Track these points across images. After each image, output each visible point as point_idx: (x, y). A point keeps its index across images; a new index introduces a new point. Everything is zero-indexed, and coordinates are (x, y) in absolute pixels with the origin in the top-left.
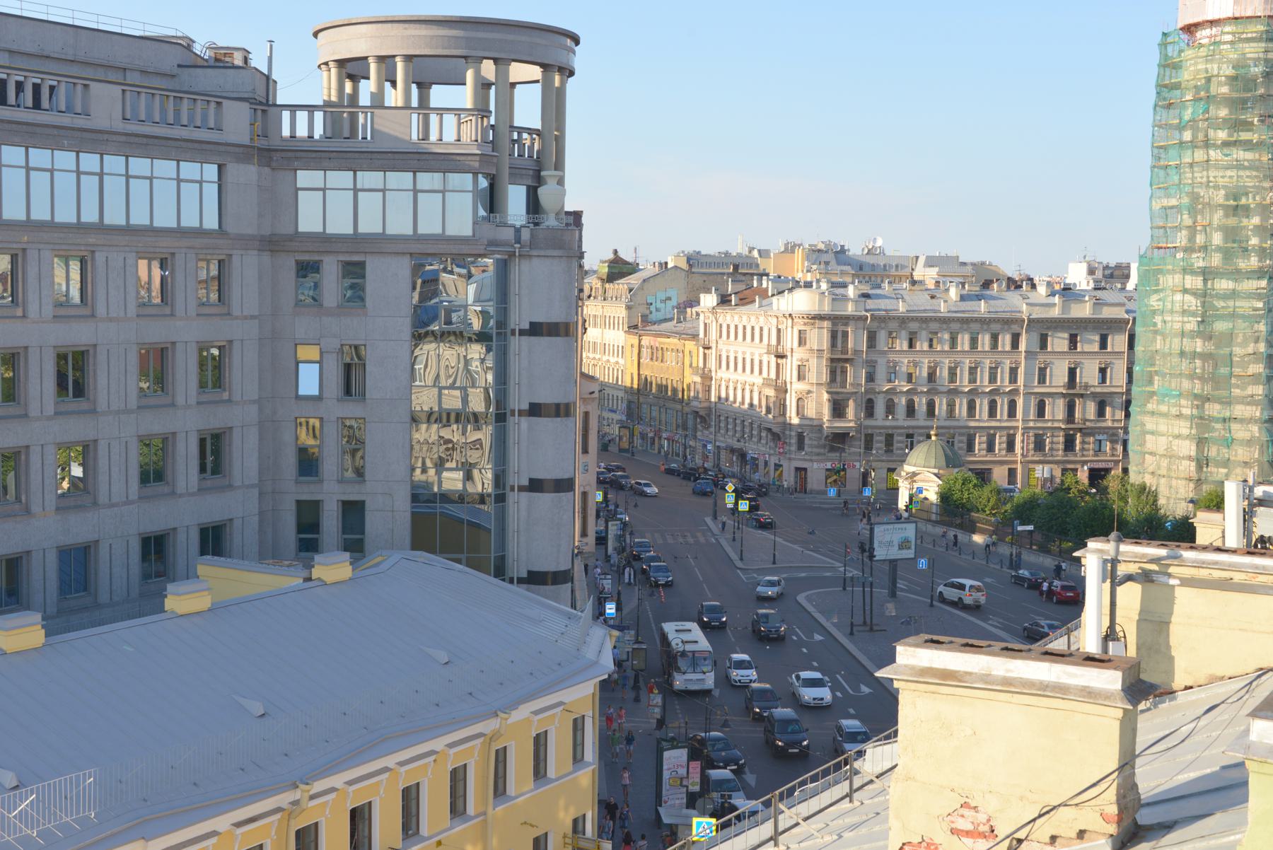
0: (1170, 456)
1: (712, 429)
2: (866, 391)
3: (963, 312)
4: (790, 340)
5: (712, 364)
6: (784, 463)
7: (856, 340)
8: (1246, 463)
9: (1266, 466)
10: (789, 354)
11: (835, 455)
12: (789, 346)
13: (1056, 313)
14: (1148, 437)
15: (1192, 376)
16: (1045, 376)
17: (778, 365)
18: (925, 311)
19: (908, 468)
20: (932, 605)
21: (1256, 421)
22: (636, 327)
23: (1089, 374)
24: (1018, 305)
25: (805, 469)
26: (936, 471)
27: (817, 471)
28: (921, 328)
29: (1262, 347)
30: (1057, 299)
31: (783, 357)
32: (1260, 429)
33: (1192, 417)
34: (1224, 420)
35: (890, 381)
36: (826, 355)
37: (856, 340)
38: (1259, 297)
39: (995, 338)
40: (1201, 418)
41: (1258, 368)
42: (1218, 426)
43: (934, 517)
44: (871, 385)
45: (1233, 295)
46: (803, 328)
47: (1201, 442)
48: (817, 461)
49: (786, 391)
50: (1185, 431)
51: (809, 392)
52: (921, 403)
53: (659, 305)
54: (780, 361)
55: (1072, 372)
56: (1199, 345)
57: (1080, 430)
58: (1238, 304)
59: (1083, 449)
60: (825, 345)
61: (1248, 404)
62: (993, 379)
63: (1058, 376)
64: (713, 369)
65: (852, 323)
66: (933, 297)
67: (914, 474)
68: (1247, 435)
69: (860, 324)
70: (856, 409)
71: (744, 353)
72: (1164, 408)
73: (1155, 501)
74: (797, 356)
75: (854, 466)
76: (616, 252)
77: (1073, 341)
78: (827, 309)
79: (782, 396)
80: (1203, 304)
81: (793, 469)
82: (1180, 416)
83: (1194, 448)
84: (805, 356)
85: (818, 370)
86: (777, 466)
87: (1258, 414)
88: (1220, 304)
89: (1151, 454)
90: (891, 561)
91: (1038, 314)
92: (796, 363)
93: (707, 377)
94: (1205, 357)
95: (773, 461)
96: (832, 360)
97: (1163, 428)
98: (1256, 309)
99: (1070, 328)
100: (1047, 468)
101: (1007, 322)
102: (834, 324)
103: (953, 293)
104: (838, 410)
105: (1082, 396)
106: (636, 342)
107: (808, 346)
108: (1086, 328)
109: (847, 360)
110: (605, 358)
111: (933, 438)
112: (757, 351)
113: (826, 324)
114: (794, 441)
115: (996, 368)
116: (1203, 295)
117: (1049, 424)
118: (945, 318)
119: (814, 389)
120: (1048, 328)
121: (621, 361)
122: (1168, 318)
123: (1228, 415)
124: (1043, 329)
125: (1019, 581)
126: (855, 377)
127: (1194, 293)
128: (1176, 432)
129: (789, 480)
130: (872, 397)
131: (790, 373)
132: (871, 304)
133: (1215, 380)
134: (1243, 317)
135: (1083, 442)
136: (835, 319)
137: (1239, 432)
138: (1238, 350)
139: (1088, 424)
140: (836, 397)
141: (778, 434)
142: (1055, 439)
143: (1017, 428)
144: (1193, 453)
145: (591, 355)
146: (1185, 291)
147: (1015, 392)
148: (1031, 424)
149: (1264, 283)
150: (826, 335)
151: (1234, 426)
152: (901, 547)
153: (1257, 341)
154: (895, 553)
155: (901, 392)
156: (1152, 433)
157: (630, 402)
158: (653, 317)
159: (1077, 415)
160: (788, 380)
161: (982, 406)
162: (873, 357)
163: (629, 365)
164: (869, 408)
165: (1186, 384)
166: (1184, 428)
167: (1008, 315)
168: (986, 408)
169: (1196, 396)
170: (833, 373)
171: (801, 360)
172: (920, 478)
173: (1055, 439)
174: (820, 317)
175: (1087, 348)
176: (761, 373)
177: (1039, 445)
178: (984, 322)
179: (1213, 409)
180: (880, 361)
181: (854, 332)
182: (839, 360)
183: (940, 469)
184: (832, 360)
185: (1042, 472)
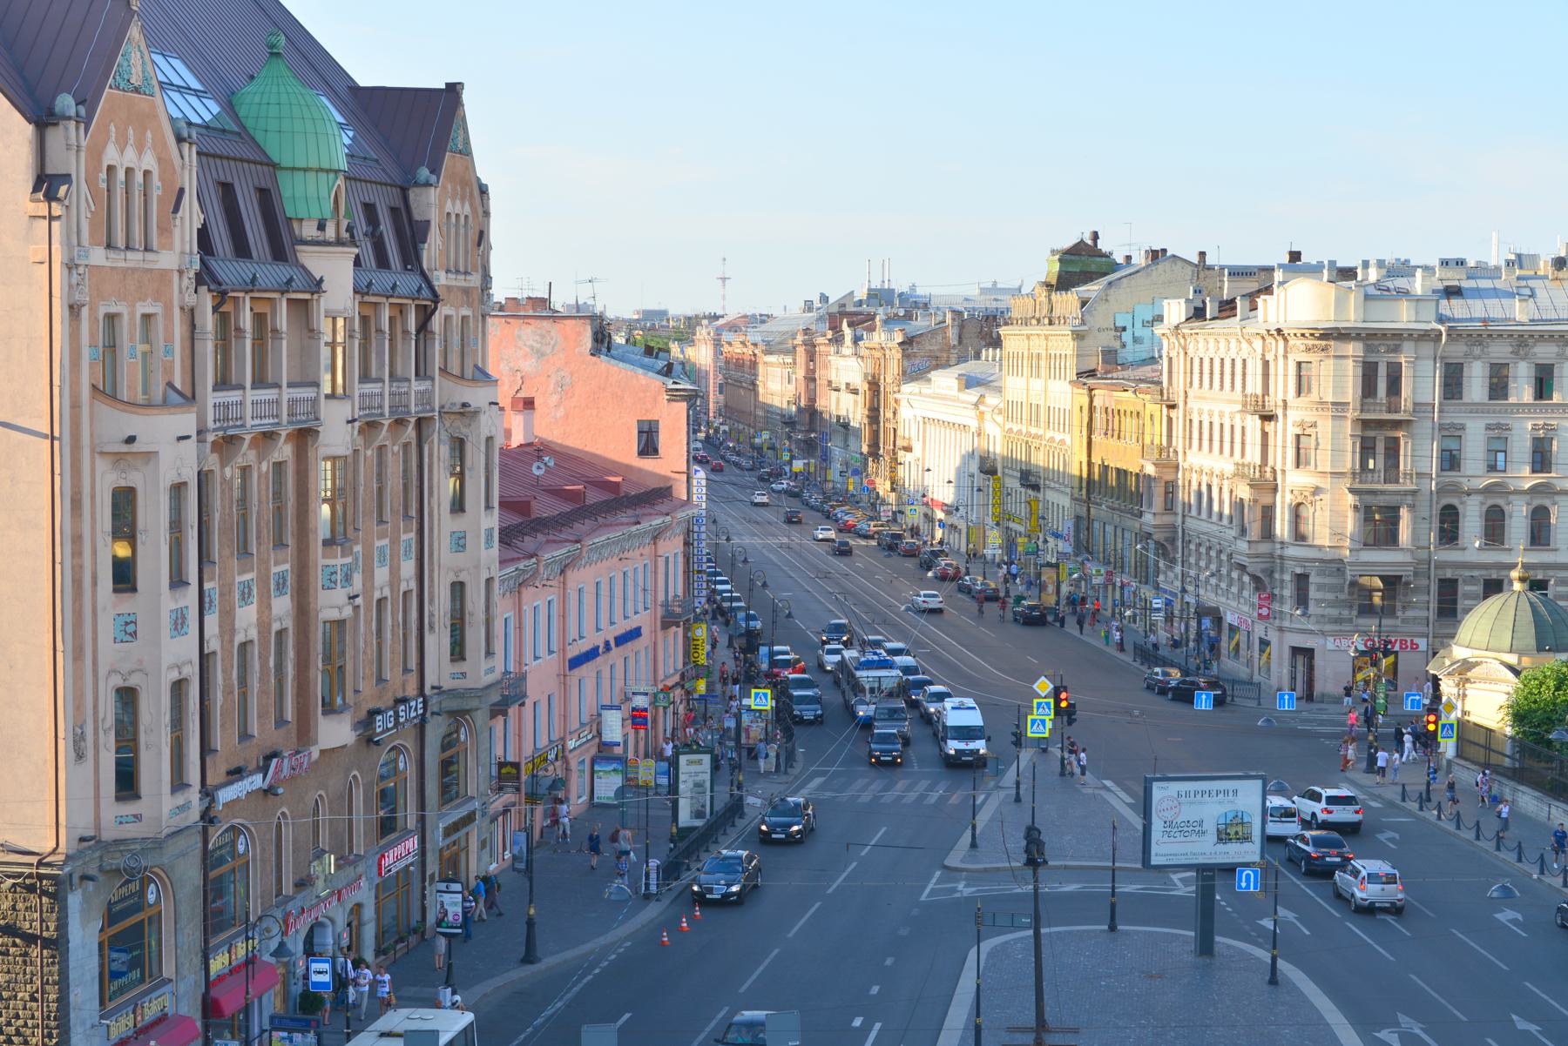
1: (1178, 569)
4: (1283, 385)
5: (1178, 442)
6: (1273, 637)
10: (1280, 412)
11: (1372, 624)
12: (1280, 397)
17: (1265, 435)
19: (1459, 652)
20: (1273, 980)
22: (1092, 373)
25: (1308, 653)
26: (1512, 659)
27: (1337, 655)
31: (1267, 418)
35: (1492, 468)
36: (1351, 414)
37: (1421, 383)
43: (1507, 762)
44: (1451, 476)
46: (1303, 357)
48: (1335, 634)
49: (1275, 489)
51: (1317, 491)
53: (1140, 331)
54: (1270, 427)
60: (1351, 392)
64: (1180, 450)
65: (1408, 347)
67: (1467, 666)
69: (1427, 348)
70: (1415, 521)
71: (1221, 416)
74: (1294, 415)
75: (1414, 647)
76: (1095, 236)
78: (1352, 317)
79: (1266, 500)
81: (1287, 654)
84: (1309, 417)
85: (1335, 445)
86: (1264, 643)
90: (1202, 869)
92: (1292, 431)
93: (1168, 463)
95: (1259, 631)
96: (1365, 424)
102: (1369, 349)
104: (1379, 524)
106: (1085, 401)
107: (1314, 396)
109: (1397, 424)
110: (1049, 434)
112: (1216, 405)
113: (1353, 349)
114: (1288, 592)
119: (1325, 483)
121: (1068, 442)
126: (1419, 456)
129: (1280, 668)
130: (1455, 501)
131: (1281, 455)
136: (1369, 337)
140: (1369, 499)
141: (1276, 574)
145: (1033, 430)
150: (1351, 374)
152: (1223, 836)
154: (1209, 851)
157: (1078, 518)
158: (1128, 354)
160: (1278, 468)
163: (1076, 448)
170: (1367, 449)
171: (1301, 424)
176: (1232, 454)
181: (1413, 364)
182: (1381, 424)
183: (1521, 654)
184: (1365, 424)
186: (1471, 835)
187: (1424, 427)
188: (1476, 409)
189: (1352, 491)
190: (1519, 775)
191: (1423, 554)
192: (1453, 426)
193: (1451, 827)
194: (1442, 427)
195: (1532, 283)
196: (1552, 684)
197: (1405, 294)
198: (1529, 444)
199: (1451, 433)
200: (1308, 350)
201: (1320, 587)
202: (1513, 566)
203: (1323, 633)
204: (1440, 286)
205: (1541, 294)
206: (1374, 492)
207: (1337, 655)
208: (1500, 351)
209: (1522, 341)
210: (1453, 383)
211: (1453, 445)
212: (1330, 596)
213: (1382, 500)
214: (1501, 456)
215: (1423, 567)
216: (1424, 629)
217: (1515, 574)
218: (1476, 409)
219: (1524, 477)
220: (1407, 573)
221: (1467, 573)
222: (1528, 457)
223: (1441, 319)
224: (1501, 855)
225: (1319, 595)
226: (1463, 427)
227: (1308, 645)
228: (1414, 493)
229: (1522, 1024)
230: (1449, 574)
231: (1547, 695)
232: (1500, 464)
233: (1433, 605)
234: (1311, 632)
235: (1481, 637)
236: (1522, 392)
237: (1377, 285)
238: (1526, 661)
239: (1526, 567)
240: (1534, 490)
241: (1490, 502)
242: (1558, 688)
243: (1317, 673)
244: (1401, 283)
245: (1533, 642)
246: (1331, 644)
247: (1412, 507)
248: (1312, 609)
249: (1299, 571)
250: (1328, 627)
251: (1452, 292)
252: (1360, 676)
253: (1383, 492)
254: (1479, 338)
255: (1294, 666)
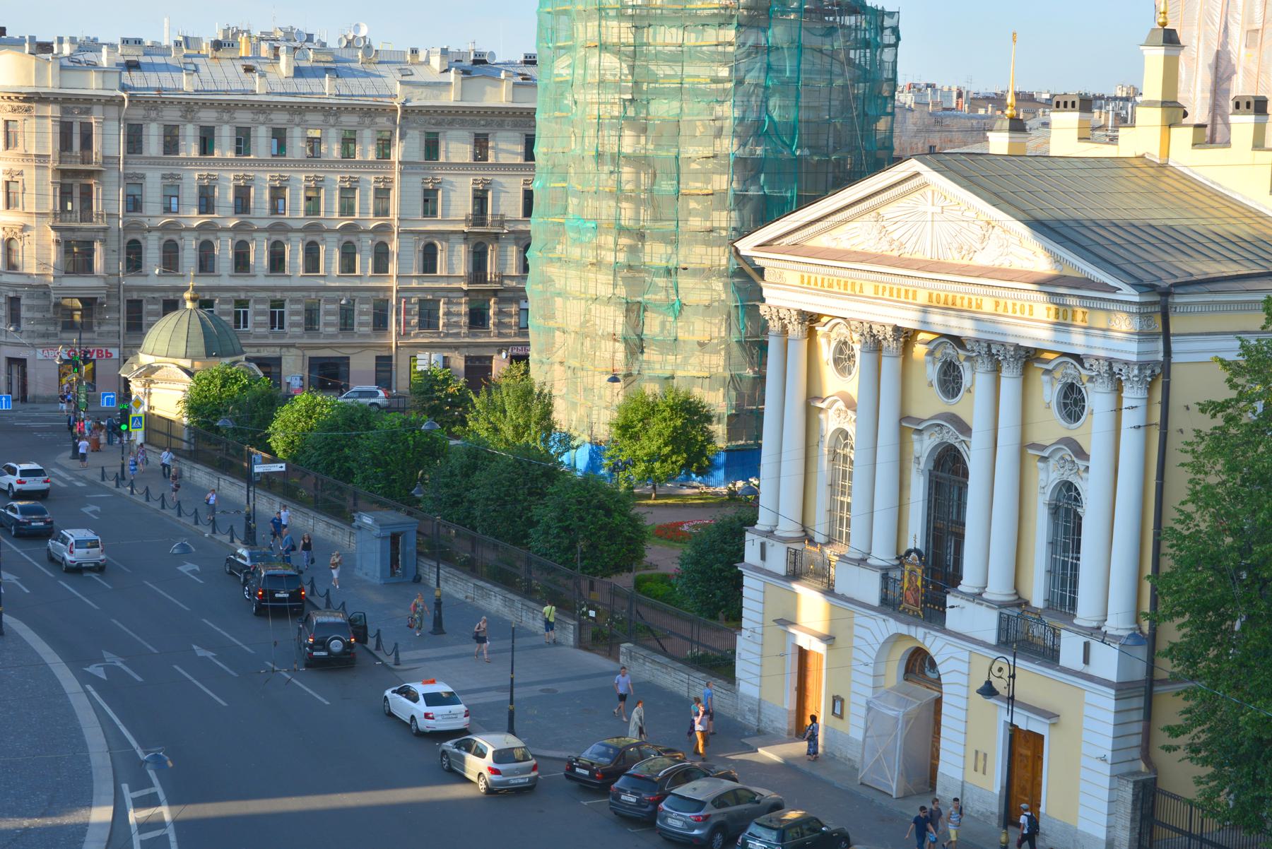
0: (585, 333)
2: (128, 228)
3: (294, 94)
7: (108, 140)
8: (701, 345)
9: (736, 350)
11: (74, 338)
13: (450, 98)
14: (559, 301)
15: (618, 195)
16: (435, 201)
18: (226, 92)
19: (145, 359)
21: (720, 274)
23: (507, 203)
24: (394, 90)
25: (22, 362)
26: (187, 363)
27: (46, 362)
28: (220, 120)
29: (728, 145)
30: (452, 76)
32: (725, 285)
33: (616, 268)
34: (668, 272)
35: (168, 210)
36: (52, 164)
37: (108, 140)
38: (724, 59)
39: (348, 142)
40: (630, 267)
41: (722, 182)
42: (661, 281)
43: (185, 446)
44: (135, 217)
45: (679, 56)
46: (10, 116)
47: (635, 311)
48: (43, 346)
50: (605, 290)
51: (24, 228)
52: (224, 251)
55: (480, 199)
56: (629, 144)
57: (495, 293)
58: (689, 70)
59: (499, 325)
60: (50, 146)
61: (707, 243)
62: (347, 209)
63: (458, 203)
65: (97, 110)
66: (249, 69)
67: (151, 369)
68: (705, 298)
69: (113, 111)
70: (106, 253)
72: (575, 252)
73: (547, 413)
75: (109, 355)
77: (481, 144)
78: (50, 84)
80: (632, 68)
82: (598, 264)
83: (621, 319)
84: (17, 167)
87: (724, 262)
88: (662, 70)
89: (558, 329)
91: (420, 99)
94: (640, 162)
96: (64, 173)
97: (574, 285)
98: (716, 80)
99: (474, 124)
100: (436, 357)
101: (370, 112)
102: (65, 111)
103: (284, 65)
104: (77, 255)
105: (496, 237)
107: (20, 149)
108: (501, 125)
109: (90, 174)
111: (189, 305)
113: (51, 110)
115: (353, 189)
116: (635, 55)
117: (443, 285)
118: (260, 104)
119: (32, 222)
120: (438, 124)
122: (579, 97)
123: (672, 264)
124: (432, 126)
125: (234, 568)
126: (108, 200)
127: (616, 49)
128: (592, 291)
130: (138, 237)
132: (136, 79)
133: (650, 200)
134: (696, 93)
135: (500, 313)
136: (65, 102)
137: (695, 292)
138: (692, 150)
139: (508, 283)
140: (68, 235)
142: (454, 309)
143: (389, 289)
144: (620, 329)
146: (603, 47)
147: (385, 229)
148: (414, 284)
149: (730, 34)
150: (50, 131)
151: (685, 282)
153: (719, 133)
155: (189, 229)
156: (559, 295)
159: (491, 268)
161: (330, 258)
162: (137, 168)
164: (134, 256)
165: (607, 208)
166: (602, 284)
167: (370, 101)
168: (337, 255)
169: (622, 230)
170: (65, 194)
171: (10, 172)
172: (165, 379)
173: (454, 309)
174: (34, 99)
175: (504, 159)
177: (428, 318)
178: (330, 112)
179: (656, 254)
180: (149, 174)
182: (76, 173)
183: (194, 359)
184: (64, 173)
185: (426, 361)
186: (157, 506)
187: (112, 176)
188: (153, 161)
189: (54, 228)
190: (194, 456)
191: (114, 280)
192: (136, 175)
193: (142, 500)
194: (126, 176)
195: (195, 60)
196: (218, 382)
197: (93, 66)
198: (196, 190)
199: (134, 182)
200: (14, 110)
201: (30, 308)
202: (186, 289)
203: (33, 346)
204: (122, 60)
205: (203, 69)
206: (72, 229)
207: (46, 362)
208: (172, 115)
209: (189, 107)
210: (134, 141)
211: (136, 191)
212: (38, 315)
213: (79, 236)
214: (174, 200)
215: (114, 290)
216: (116, 341)
217: (187, 295)
218: (153, 161)
219: (194, 218)
220: (101, 295)
221: (150, 295)
222: (195, 201)
223: (123, 88)
224: (182, 520)
225: (29, 315)
226: (143, 177)
227: (21, 356)
228: (105, 230)
229: (201, 652)
230: (135, 296)
231: (215, 391)
232: (174, 207)
233: (123, 321)
234: (23, 345)
235: (162, 346)
236: (190, 149)
237: (70, 58)
238: (198, 365)
239: (196, 289)
240: (201, 228)
241: (167, 237)
242: (223, 386)
243: (30, 379)
244: (90, 56)
245: (202, 350)
246: (40, 354)
247: (104, 242)
248: (24, 326)
249: (11, 294)
250: (37, 341)
251: (132, 66)
252: (64, 381)
253: (79, 229)
254: (154, 103)
255: (10, 374)
